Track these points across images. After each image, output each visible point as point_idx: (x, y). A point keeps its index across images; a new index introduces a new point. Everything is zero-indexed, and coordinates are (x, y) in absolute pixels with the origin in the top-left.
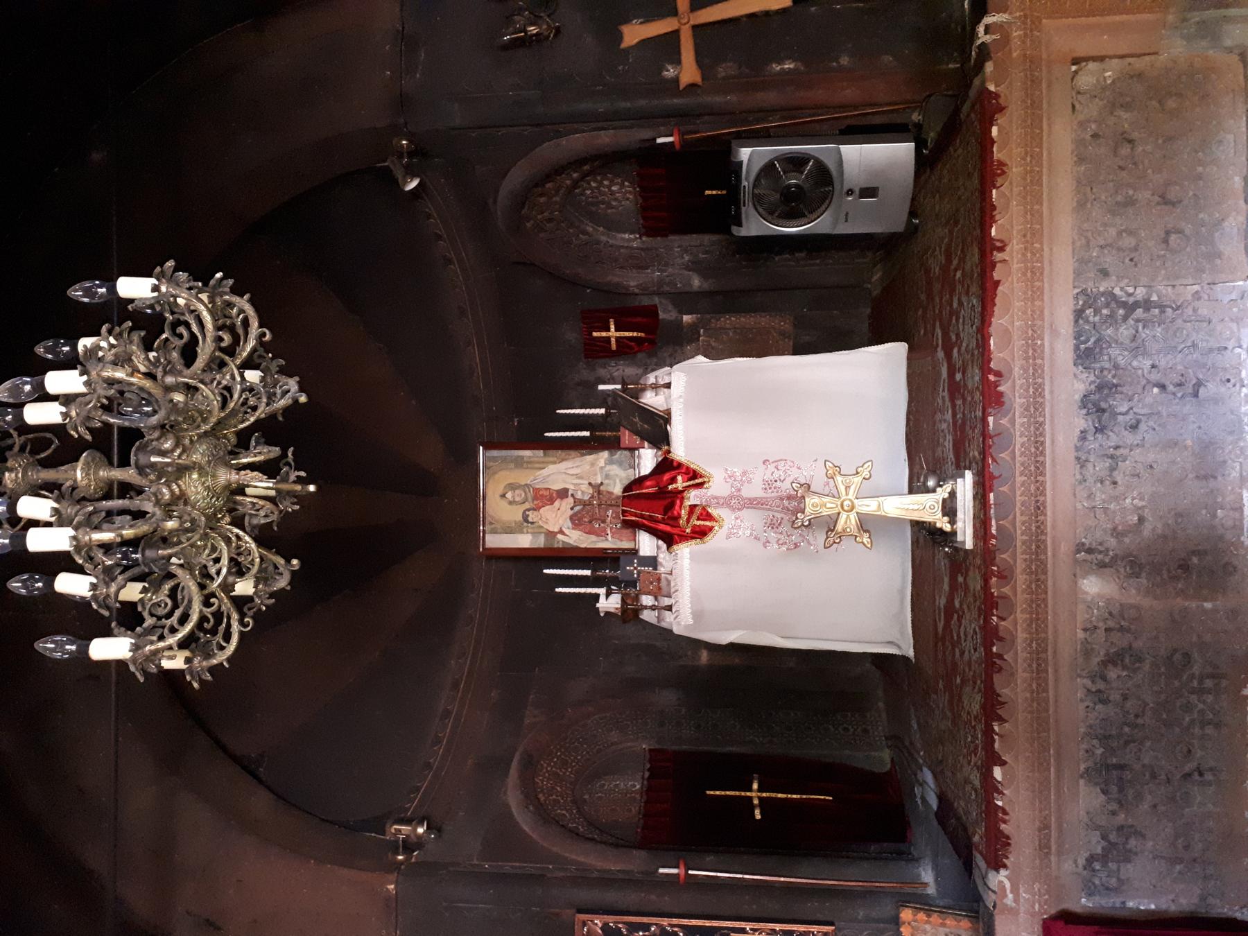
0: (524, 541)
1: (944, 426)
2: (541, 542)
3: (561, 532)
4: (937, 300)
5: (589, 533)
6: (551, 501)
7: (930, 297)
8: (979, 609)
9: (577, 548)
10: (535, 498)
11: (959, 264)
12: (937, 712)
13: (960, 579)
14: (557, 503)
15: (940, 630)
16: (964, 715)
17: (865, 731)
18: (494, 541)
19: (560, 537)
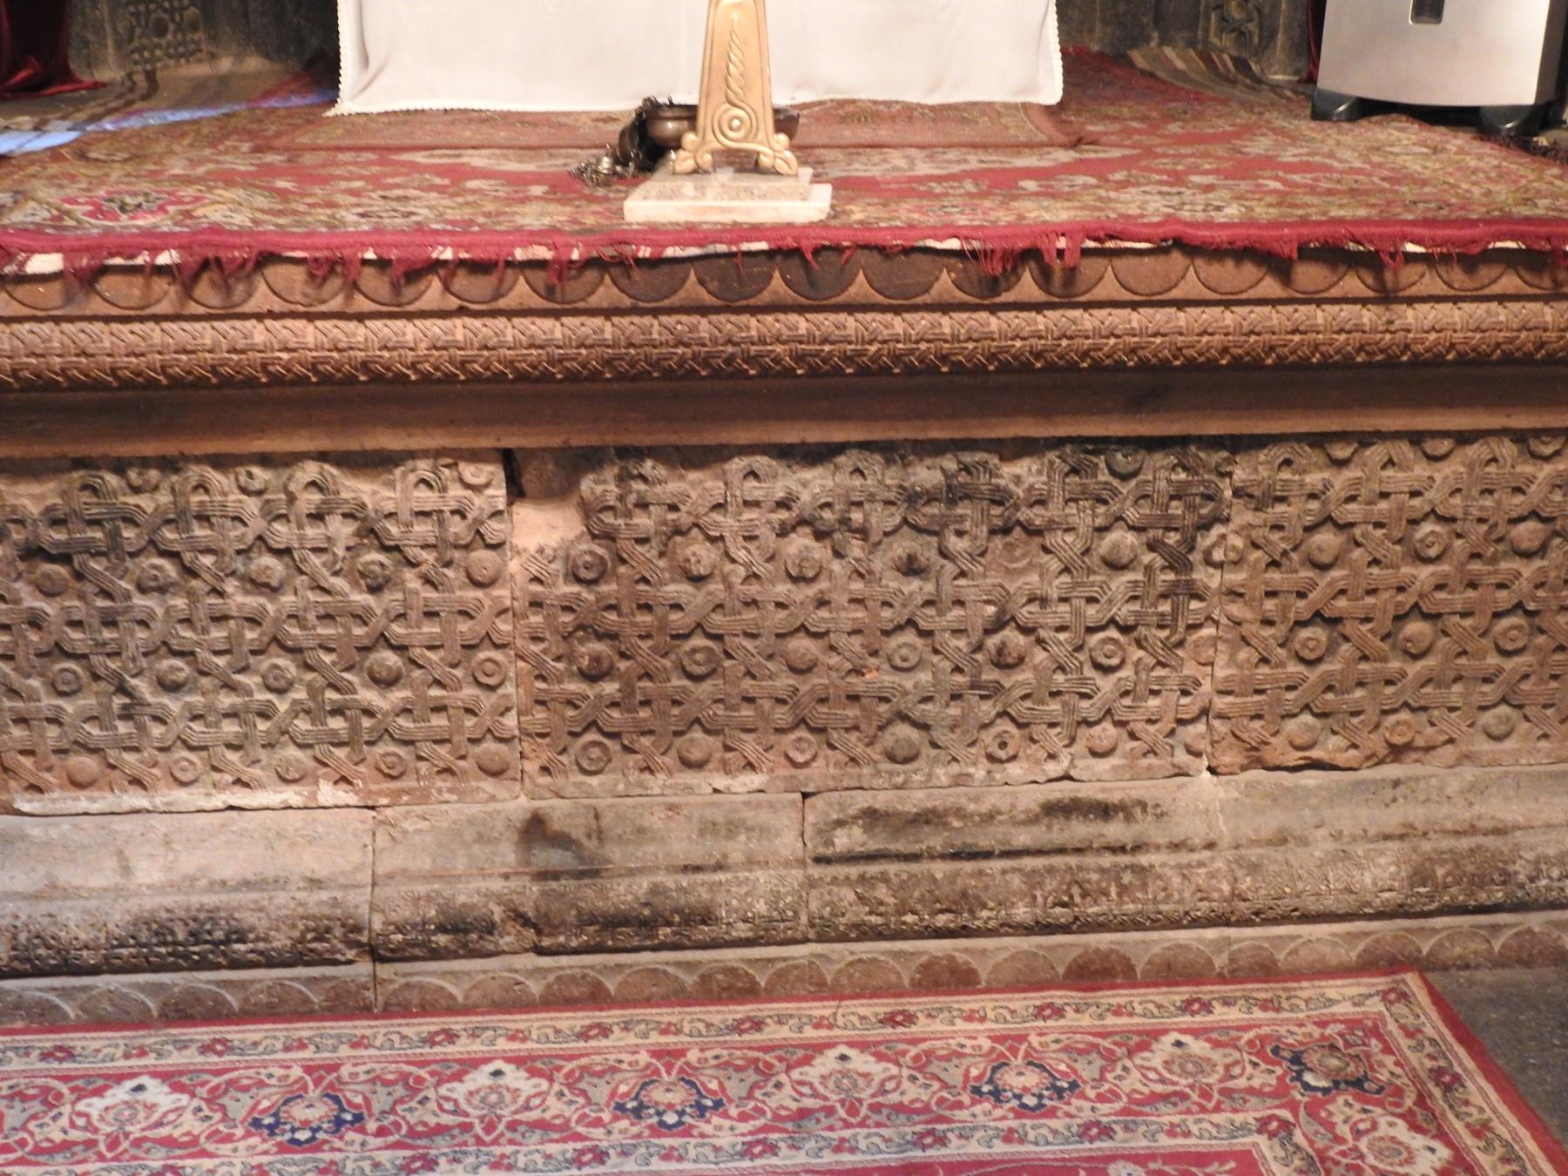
1: (902, 163)
4: (1189, 150)
7: (1180, 140)
8: (471, 222)
11: (1298, 186)
12: (208, 152)
13: (537, 190)
15: (406, 157)
16: (188, 192)
17: (161, 30)
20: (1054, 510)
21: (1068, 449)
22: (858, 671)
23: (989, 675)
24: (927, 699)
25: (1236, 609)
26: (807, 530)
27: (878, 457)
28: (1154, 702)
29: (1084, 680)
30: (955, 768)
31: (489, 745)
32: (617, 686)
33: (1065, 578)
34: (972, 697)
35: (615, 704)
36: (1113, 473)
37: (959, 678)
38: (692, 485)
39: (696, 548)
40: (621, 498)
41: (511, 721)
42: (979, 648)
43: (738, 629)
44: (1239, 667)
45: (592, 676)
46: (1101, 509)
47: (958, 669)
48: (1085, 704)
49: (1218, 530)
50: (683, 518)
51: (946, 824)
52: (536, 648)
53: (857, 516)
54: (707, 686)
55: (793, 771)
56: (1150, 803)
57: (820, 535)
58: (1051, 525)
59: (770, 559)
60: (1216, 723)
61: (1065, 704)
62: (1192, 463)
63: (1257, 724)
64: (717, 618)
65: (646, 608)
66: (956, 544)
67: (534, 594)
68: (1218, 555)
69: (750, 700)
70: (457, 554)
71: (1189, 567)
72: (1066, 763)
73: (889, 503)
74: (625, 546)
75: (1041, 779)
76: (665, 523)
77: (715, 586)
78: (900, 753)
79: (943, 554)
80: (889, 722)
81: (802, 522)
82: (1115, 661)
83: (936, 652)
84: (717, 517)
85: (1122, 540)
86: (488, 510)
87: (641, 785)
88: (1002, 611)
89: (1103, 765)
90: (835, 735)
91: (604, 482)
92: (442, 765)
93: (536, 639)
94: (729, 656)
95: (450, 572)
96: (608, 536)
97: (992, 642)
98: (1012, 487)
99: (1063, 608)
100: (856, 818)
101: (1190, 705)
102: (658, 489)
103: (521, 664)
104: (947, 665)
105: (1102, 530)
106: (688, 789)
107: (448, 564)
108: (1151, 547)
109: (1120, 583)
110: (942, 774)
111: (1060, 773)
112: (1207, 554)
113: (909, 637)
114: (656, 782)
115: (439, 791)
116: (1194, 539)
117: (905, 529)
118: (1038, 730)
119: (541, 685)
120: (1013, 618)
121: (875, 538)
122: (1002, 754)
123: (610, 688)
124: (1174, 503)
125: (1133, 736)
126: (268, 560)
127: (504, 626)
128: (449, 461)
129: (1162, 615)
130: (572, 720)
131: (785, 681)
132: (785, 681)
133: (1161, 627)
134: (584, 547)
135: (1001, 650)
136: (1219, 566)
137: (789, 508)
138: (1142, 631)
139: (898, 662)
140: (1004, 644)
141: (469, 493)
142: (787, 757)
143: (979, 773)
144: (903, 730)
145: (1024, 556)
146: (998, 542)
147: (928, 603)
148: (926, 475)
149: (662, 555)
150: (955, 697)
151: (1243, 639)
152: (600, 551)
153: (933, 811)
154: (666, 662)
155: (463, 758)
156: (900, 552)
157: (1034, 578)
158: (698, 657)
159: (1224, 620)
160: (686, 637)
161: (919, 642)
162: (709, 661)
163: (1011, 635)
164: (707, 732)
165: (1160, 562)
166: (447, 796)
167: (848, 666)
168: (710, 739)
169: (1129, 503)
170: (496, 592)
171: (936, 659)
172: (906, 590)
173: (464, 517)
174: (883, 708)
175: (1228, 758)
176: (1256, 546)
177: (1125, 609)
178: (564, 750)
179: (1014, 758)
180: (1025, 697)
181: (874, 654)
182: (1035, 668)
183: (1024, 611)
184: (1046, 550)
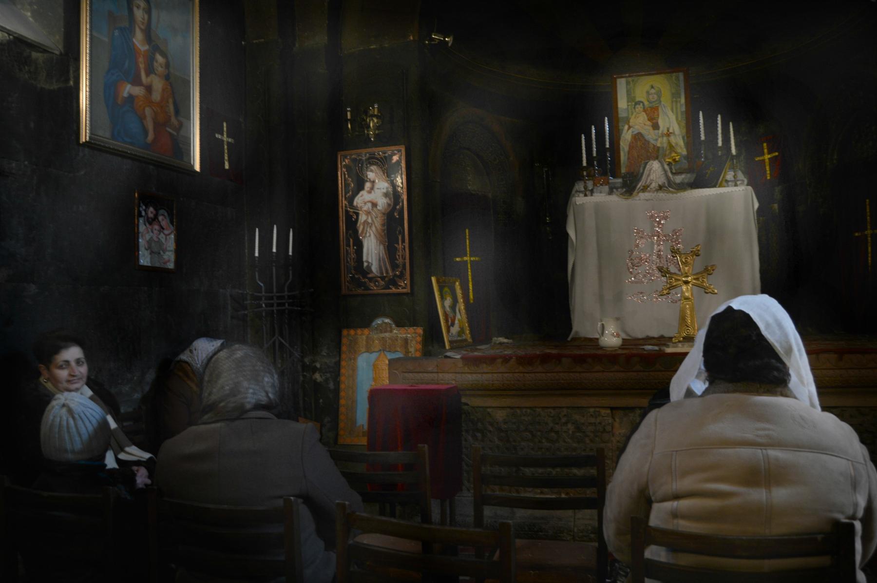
0: (622, 103)
2: (622, 114)
3: (630, 127)
5: (630, 146)
6: (650, 119)
9: (619, 139)
10: (652, 108)
14: (649, 123)
18: (622, 85)
19: (626, 127)
126: (553, 434)
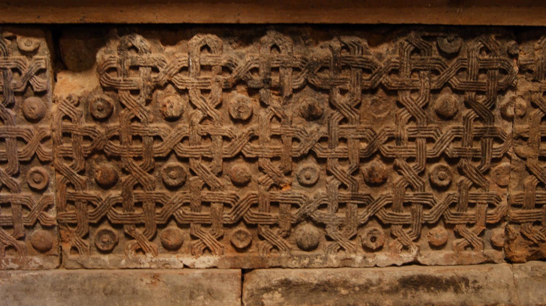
20: (405, 77)
21: (412, 34)
22: (277, 186)
23: (364, 190)
24: (323, 206)
25: (522, 149)
26: (243, 88)
27: (288, 38)
28: (471, 212)
29: (426, 196)
30: (342, 254)
31: (38, 231)
32: (120, 192)
33: (412, 125)
34: (353, 206)
35: (118, 205)
36: (441, 52)
37: (344, 192)
38: (168, 55)
39: (170, 98)
40: (120, 62)
41: (52, 215)
42: (356, 172)
43: (198, 154)
44: (524, 188)
45: (105, 186)
46: (435, 78)
47: (343, 186)
48: (426, 212)
49: (510, 95)
50: (162, 77)
51: (336, 292)
52: (67, 165)
53: (275, 79)
54: (179, 194)
55: (237, 254)
56: (471, 279)
57: (252, 92)
58: (402, 88)
59: (218, 107)
60: (512, 227)
61: (413, 212)
62: (492, 46)
63: (537, 228)
64: (185, 147)
65: (138, 138)
66: (340, 99)
67: (65, 127)
68: (510, 111)
69: (207, 204)
70: (17, 100)
71: (492, 119)
72: (415, 253)
73: (296, 69)
74: (124, 95)
75: (399, 263)
76: (149, 80)
77: (183, 126)
78: (307, 243)
79: (333, 106)
80: (299, 222)
81: (240, 82)
82: (445, 183)
83: (329, 174)
84: (183, 76)
85: (448, 98)
86: (35, 69)
87: (136, 261)
88: (371, 146)
89: (439, 255)
90: (263, 230)
91: (111, 52)
92: (8, 243)
93: (68, 159)
94: (194, 174)
95: (12, 112)
96: (111, 88)
97: (365, 168)
98: (376, 60)
99: (411, 145)
100: (276, 287)
101: (495, 214)
102: (145, 56)
103: (59, 176)
104: (336, 183)
105: (436, 92)
106: (166, 265)
107: (11, 106)
108: (468, 105)
109: (448, 129)
110: (334, 258)
111: (411, 259)
112: (503, 110)
113: (311, 163)
114: (146, 260)
115: (7, 261)
116: (495, 99)
117: (307, 88)
118: (396, 229)
119: (71, 191)
120: (378, 152)
121: (287, 93)
122: (373, 245)
123: (115, 193)
124: (482, 76)
125: (458, 235)
127: (46, 149)
128: (9, 34)
129: (476, 151)
130: (92, 215)
131: (229, 191)
132: (230, 191)
133: (475, 160)
134: (98, 96)
135: (371, 172)
136: (510, 119)
137: (231, 72)
138: (463, 162)
139: (304, 180)
140: (373, 168)
141: (23, 57)
142: (233, 245)
143: (359, 258)
144: (308, 228)
145: (385, 109)
146: (368, 99)
147: (323, 140)
148: (320, 52)
149: (148, 102)
150: (342, 205)
151: (528, 169)
152: (108, 99)
153: (328, 283)
154: (152, 177)
155: (22, 239)
156: (304, 104)
157: (393, 125)
158: (172, 173)
159: (514, 157)
160: (165, 159)
161: (318, 167)
162: (180, 177)
163: (377, 163)
164: (181, 226)
165: (473, 115)
166: (11, 265)
167: (271, 181)
168: (182, 231)
169: (452, 73)
170: (41, 126)
171: (328, 179)
172: (308, 130)
173: (20, 74)
174: (294, 212)
175: (520, 252)
176: (534, 105)
177: (451, 146)
178: (86, 237)
179: (380, 249)
180: (388, 206)
181: (288, 174)
182: (394, 186)
183: (386, 146)
184: (400, 105)
